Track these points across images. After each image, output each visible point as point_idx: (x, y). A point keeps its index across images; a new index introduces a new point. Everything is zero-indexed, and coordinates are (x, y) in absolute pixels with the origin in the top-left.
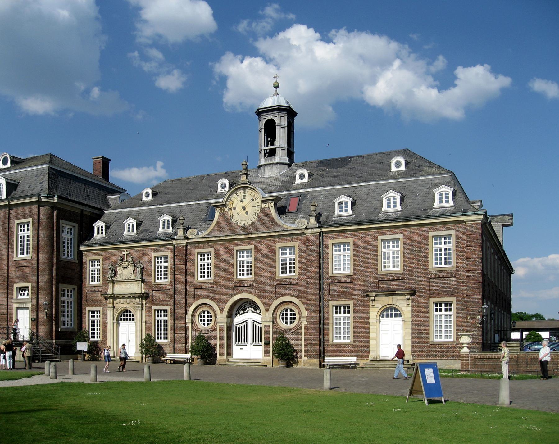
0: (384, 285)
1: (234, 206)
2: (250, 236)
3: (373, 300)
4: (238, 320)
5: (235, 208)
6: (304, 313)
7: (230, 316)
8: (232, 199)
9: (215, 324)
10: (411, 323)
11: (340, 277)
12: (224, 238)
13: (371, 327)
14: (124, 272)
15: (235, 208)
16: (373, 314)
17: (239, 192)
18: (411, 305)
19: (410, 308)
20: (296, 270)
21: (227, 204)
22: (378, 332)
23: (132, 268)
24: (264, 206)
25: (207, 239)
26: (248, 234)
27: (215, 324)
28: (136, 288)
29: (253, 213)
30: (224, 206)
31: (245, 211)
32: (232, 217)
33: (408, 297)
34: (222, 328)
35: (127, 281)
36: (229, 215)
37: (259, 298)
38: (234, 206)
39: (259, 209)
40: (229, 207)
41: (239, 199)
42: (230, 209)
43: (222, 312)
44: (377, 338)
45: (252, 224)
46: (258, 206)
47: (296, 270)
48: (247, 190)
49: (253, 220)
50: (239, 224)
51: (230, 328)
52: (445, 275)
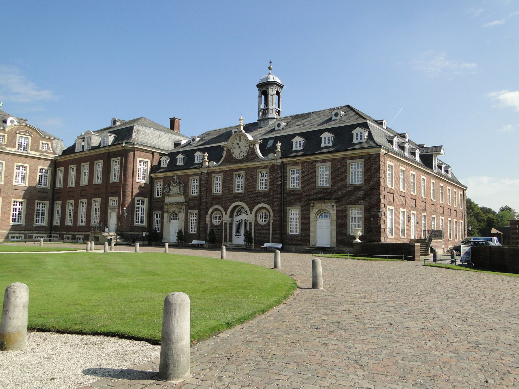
0: (319, 196)
3: (312, 206)
4: (236, 219)
6: (272, 215)
7: (231, 216)
9: (222, 221)
10: (335, 222)
11: (293, 191)
13: (311, 224)
14: (175, 189)
16: (312, 215)
18: (335, 210)
19: (335, 212)
20: (36, 211)
22: (315, 227)
23: (178, 187)
27: (222, 221)
28: (181, 199)
33: (334, 204)
34: (226, 224)
35: (175, 195)
37: (247, 204)
43: (226, 214)
44: (315, 232)
46: (247, 146)
47: (36, 211)
51: (231, 224)
52: (357, 188)
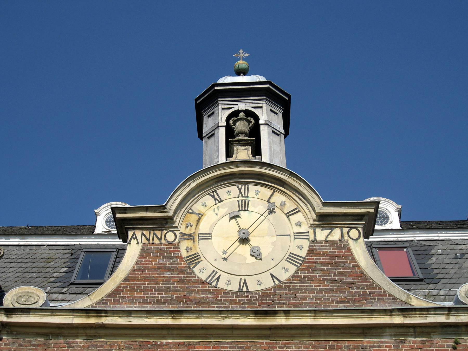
1: (203, 228)
2: (281, 321)
5: (208, 236)
8: (198, 207)
12: (168, 321)
15: (208, 236)
17: (222, 192)
21: (177, 219)
24: (321, 235)
25: (93, 321)
26: (273, 313)
29: (280, 255)
30: (165, 223)
31: (246, 249)
32: (195, 259)
36: (184, 254)
38: (203, 228)
39: (306, 244)
40: (183, 229)
41: (224, 209)
42: (190, 237)
45: (273, 290)
48: (253, 189)
49: (284, 277)
50: (221, 285)
